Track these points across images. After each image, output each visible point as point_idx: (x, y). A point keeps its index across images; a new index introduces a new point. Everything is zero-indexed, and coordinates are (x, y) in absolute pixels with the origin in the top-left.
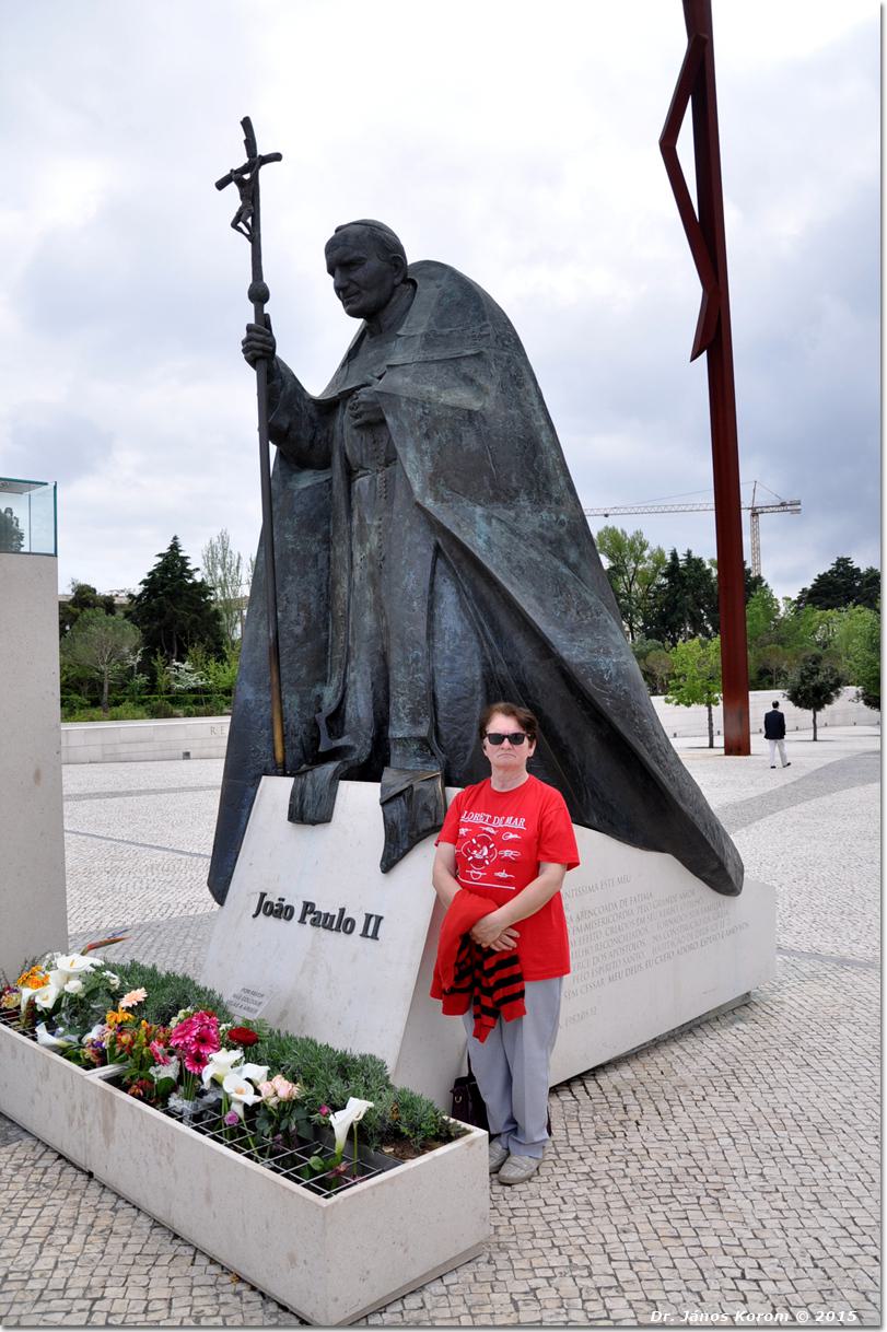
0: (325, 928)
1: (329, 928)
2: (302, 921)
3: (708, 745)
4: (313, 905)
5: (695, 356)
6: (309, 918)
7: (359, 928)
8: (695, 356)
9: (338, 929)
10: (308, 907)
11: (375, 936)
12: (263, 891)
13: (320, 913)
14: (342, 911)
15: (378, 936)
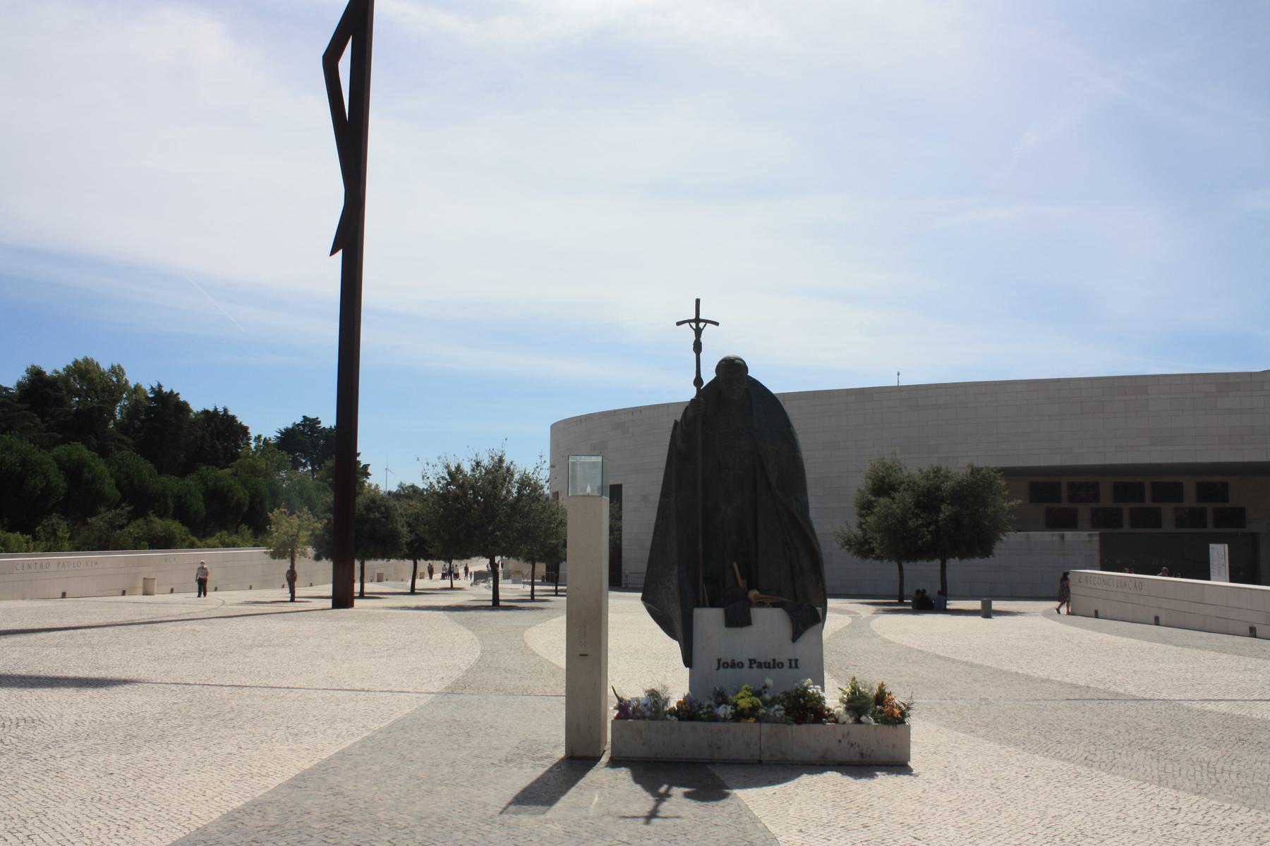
0: (766, 667)
1: (769, 667)
2: (751, 667)
3: (289, 599)
4: (755, 661)
5: (333, 252)
6: (754, 666)
7: (787, 664)
8: (333, 252)
9: (774, 667)
10: (752, 662)
11: (797, 667)
12: (719, 658)
13: (760, 663)
14: (774, 660)
15: (799, 665)
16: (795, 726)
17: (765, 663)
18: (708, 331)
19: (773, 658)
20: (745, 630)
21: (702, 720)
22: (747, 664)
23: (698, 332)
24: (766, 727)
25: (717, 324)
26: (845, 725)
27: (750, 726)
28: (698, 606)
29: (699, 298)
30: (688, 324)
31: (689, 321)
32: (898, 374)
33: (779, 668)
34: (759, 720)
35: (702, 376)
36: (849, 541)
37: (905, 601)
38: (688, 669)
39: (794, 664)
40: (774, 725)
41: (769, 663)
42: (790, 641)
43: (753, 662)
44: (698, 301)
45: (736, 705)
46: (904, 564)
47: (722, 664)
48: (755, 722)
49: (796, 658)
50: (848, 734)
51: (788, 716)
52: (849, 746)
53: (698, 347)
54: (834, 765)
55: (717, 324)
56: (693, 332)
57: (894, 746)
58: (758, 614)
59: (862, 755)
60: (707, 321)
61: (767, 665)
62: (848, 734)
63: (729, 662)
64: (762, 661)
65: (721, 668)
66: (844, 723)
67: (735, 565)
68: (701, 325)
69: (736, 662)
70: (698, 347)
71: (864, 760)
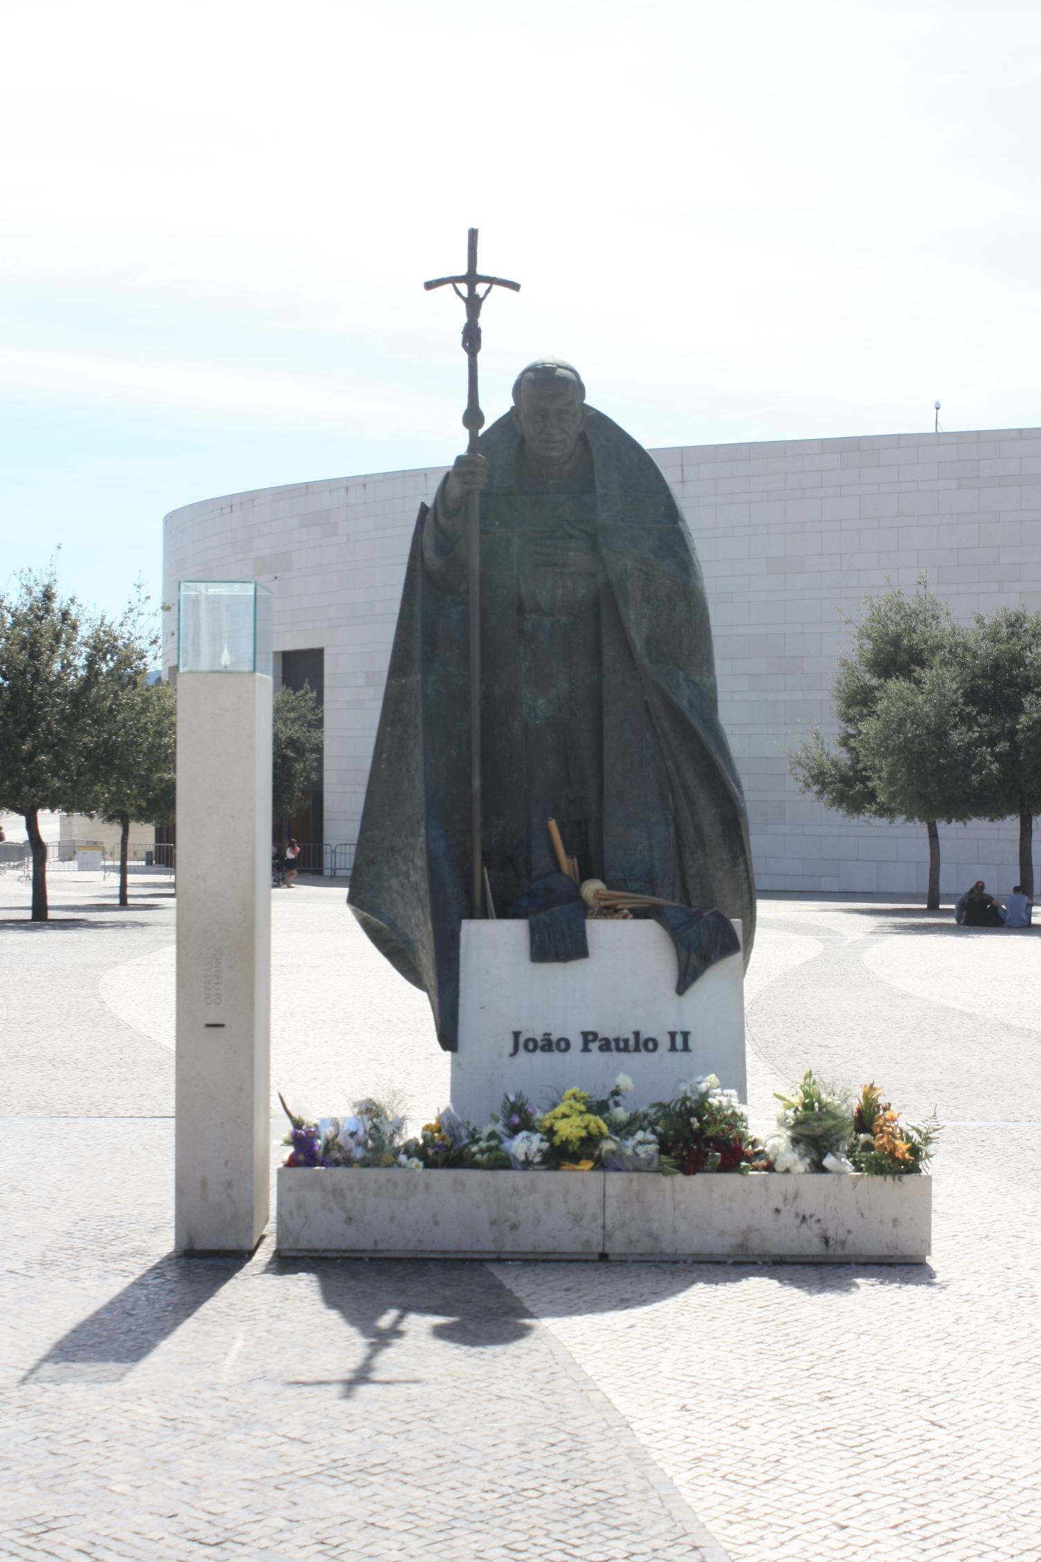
0: (618, 1049)
1: (626, 1049)
2: (586, 1049)
4: (595, 1035)
6: (594, 1046)
7: (664, 1042)
9: (637, 1049)
11: (686, 1048)
13: (607, 1040)
14: (637, 1034)
15: (691, 1045)
16: (680, 1178)
17: (617, 1040)
18: (495, 303)
19: (635, 1029)
20: (575, 968)
21: (476, 1166)
22: (577, 1042)
23: (474, 305)
24: (616, 1181)
25: (515, 286)
26: (789, 1176)
27: (580, 1179)
28: (471, 916)
29: (475, 227)
30: (449, 286)
31: (454, 280)
32: (938, 409)
33: (647, 1050)
34: (602, 1164)
35: (483, 405)
36: (822, 773)
37: (941, 906)
38: (449, 1053)
39: (681, 1041)
40: (635, 1175)
41: (626, 1041)
42: (673, 993)
43: (590, 1037)
44: (473, 234)
45: (550, 1132)
46: (941, 826)
47: (522, 1043)
48: (592, 1169)
49: (685, 1029)
50: (796, 1196)
51: (663, 1156)
52: (798, 1221)
53: (472, 339)
54: (764, 1263)
55: (515, 286)
56: (463, 305)
57: (895, 1222)
58: (599, 931)
59: (826, 1241)
60: (492, 281)
61: (622, 1045)
62: (796, 1196)
63: (539, 1037)
64: (611, 1036)
65: (522, 1052)
66: (787, 1171)
67: (553, 824)
68: (481, 289)
69: (554, 1038)
70: (472, 339)
71: (831, 1252)
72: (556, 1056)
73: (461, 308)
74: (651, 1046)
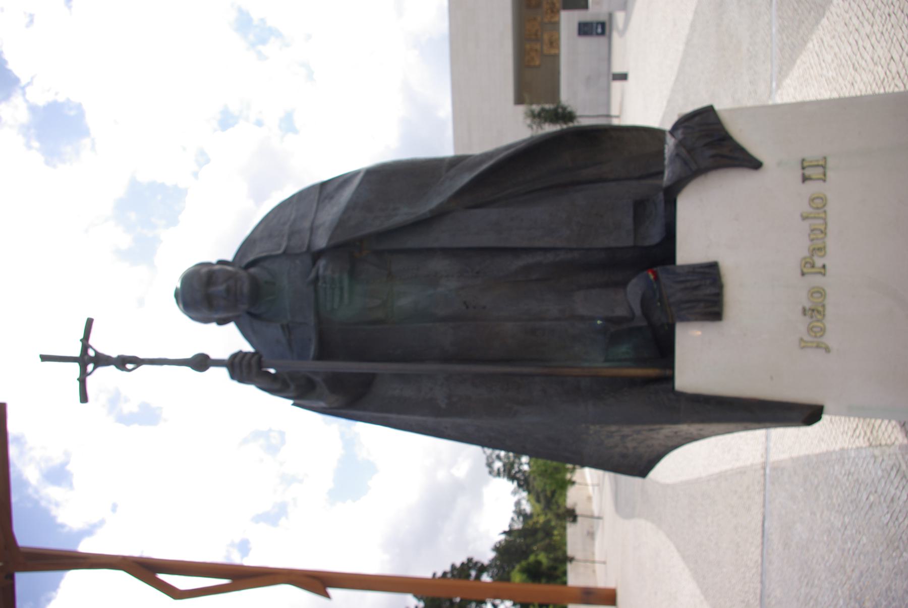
6: (819, 262)
14: (804, 218)
23: (101, 360)
25: (90, 322)
72: (830, 301)
73: (101, 370)
74: (818, 202)
